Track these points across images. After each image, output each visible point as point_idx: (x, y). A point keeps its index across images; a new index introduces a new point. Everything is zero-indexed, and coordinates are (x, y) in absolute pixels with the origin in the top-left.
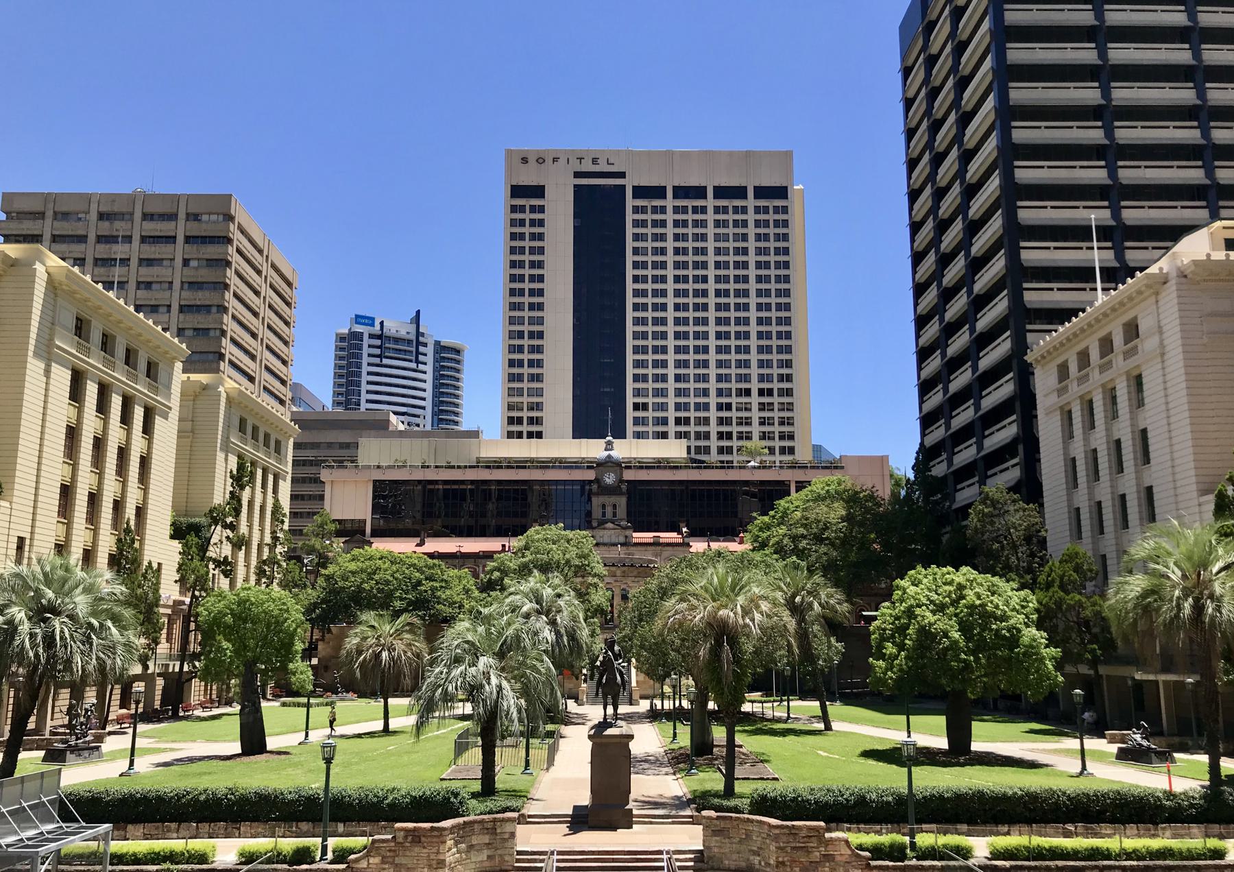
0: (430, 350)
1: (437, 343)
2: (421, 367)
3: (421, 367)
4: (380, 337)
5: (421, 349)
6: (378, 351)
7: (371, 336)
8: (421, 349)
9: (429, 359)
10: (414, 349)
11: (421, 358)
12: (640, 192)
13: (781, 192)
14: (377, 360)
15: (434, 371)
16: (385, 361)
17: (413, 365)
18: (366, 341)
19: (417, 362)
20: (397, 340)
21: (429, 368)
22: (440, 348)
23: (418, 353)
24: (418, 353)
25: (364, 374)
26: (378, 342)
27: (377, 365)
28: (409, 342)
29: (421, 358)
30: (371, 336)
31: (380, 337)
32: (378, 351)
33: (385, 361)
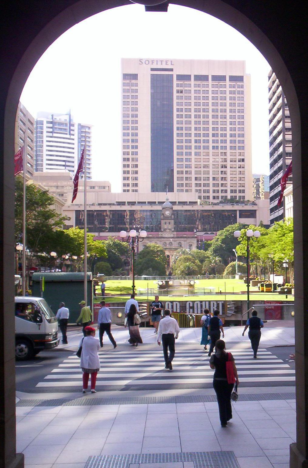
0: (76, 128)
1: (79, 125)
2: (72, 137)
3: (72, 137)
4: (51, 123)
5: (72, 128)
6: (51, 130)
7: (48, 122)
8: (72, 128)
9: (76, 132)
10: (68, 128)
11: (72, 132)
12: (180, 77)
13: (240, 79)
14: (51, 134)
15: (79, 138)
16: (55, 135)
17: (68, 136)
18: (45, 125)
19: (70, 134)
20: (60, 124)
21: (76, 137)
22: (81, 127)
23: (70, 130)
24: (70, 130)
25: (45, 141)
26: (51, 125)
27: (51, 137)
28: (66, 125)
29: (72, 132)
30: (48, 122)
31: (51, 123)
32: (51, 130)
33: (55, 135)
